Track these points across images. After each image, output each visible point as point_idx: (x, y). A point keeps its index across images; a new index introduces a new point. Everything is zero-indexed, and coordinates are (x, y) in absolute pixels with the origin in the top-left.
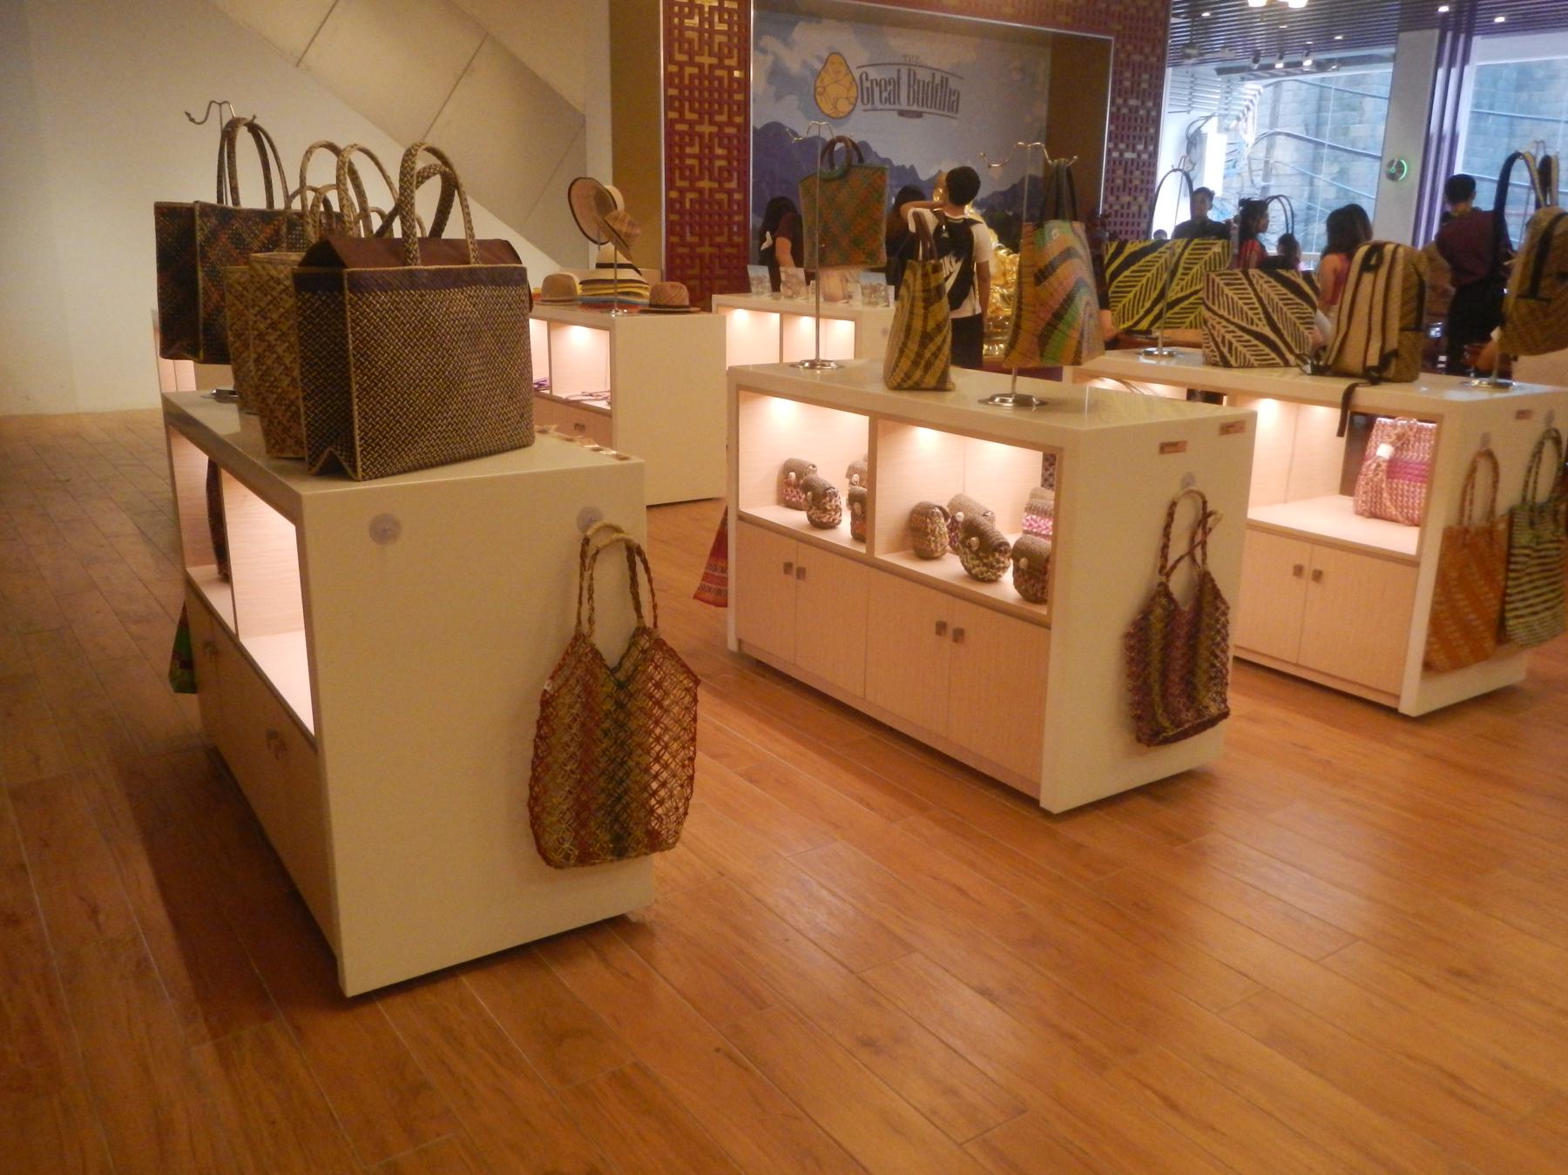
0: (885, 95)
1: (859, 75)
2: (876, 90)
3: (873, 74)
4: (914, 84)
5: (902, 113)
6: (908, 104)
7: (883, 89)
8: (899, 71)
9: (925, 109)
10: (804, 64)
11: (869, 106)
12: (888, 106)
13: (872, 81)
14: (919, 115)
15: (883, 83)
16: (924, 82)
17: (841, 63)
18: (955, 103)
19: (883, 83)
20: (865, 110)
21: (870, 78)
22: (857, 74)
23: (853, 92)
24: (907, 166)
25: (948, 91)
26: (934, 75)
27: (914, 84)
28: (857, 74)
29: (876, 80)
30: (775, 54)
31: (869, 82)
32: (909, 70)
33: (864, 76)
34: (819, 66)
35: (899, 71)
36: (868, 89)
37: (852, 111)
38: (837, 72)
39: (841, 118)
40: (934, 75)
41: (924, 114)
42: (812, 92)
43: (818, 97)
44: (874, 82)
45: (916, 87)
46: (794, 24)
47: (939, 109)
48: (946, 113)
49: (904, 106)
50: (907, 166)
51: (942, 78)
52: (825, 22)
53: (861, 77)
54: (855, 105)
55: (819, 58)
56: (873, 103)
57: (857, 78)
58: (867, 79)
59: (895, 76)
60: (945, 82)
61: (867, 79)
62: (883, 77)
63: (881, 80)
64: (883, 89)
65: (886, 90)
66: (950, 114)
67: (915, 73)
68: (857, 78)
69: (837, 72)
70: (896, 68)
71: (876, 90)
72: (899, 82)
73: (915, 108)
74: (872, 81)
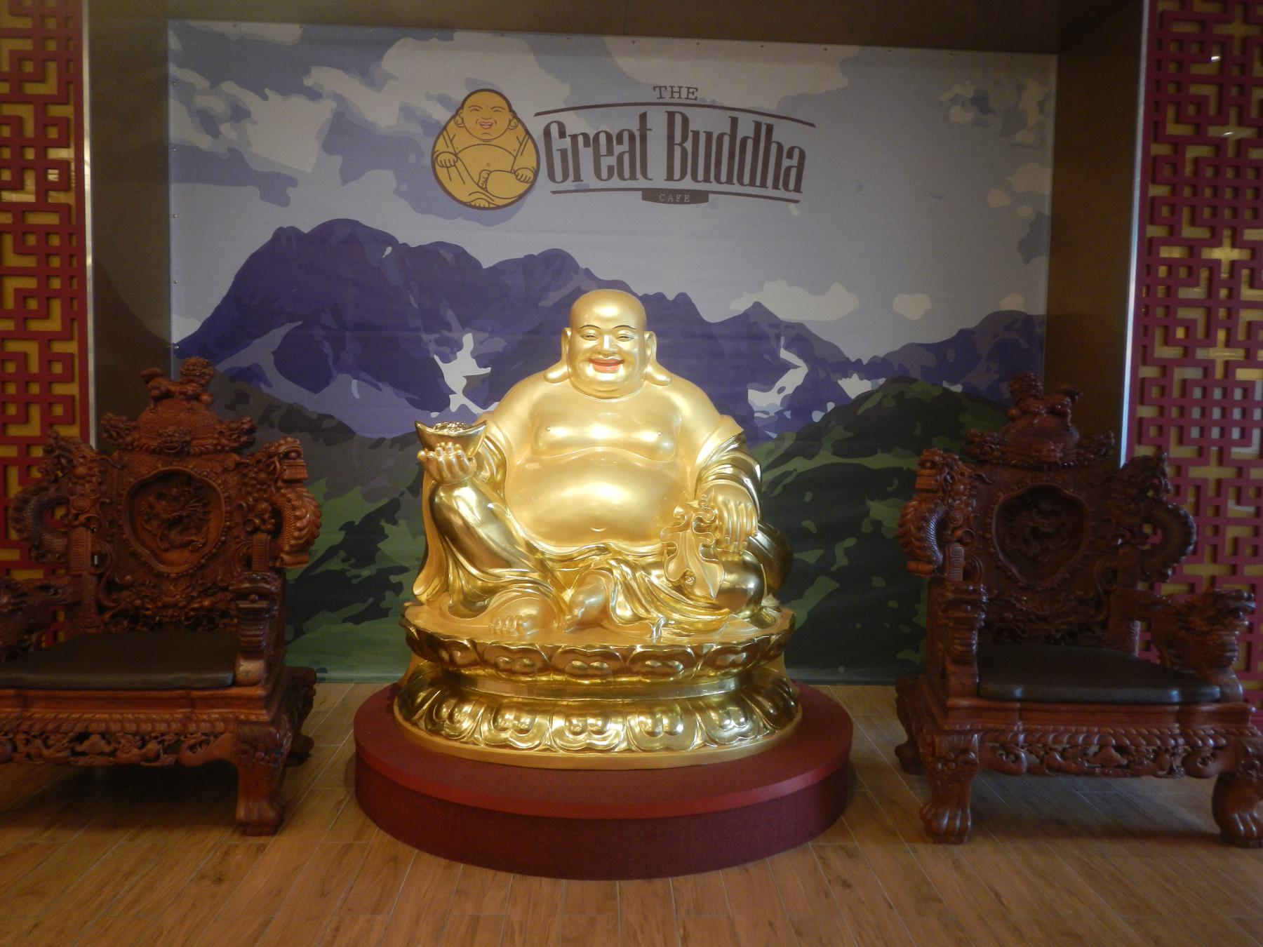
0: (607, 162)
1: (541, 129)
2: (586, 155)
3: (576, 124)
4: (684, 138)
5: (651, 195)
6: (670, 177)
7: (603, 150)
8: (643, 117)
9: (713, 186)
10: (407, 112)
11: (570, 184)
12: (615, 182)
13: (574, 138)
14: (699, 197)
15: (603, 138)
16: (709, 135)
17: (496, 109)
18: (794, 172)
19: (603, 138)
20: (554, 192)
21: (569, 131)
22: (536, 128)
23: (528, 159)
24: (671, 296)
25: (774, 148)
26: (734, 121)
27: (684, 138)
28: (536, 128)
29: (586, 136)
30: (338, 97)
31: (568, 140)
32: (671, 116)
33: (554, 130)
34: (441, 115)
35: (643, 117)
36: (564, 152)
37: (521, 196)
38: (487, 125)
39: (498, 207)
40: (734, 121)
41: (711, 196)
42: (427, 161)
43: (442, 172)
44: (581, 139)
45: (688, 145)
46: (388, 44)
47: (752, 183)
48: (769, 191)
49: (658, 178)
50: (671, 296)
51: (758, 126)
52: (459, 36)
53: (547, 133)
54: (533, 183)
55: (444, 101)
56: (577, 178)
57: (537, 133)
58: (562, 134)
59: (635, 127)
60: (763, 133)
61: (562, 134)
62: (604, 128)
63: (597, 136)
64: (603, 150)
65: (610, 152)
66: (781, 193)
67: (685, 121)
68: (537, 133)
69: (487, 125)
70: (642, 109)
71: (586, 155)
72: (644, 138)
73: (688, 184)
74: (574, 138)
